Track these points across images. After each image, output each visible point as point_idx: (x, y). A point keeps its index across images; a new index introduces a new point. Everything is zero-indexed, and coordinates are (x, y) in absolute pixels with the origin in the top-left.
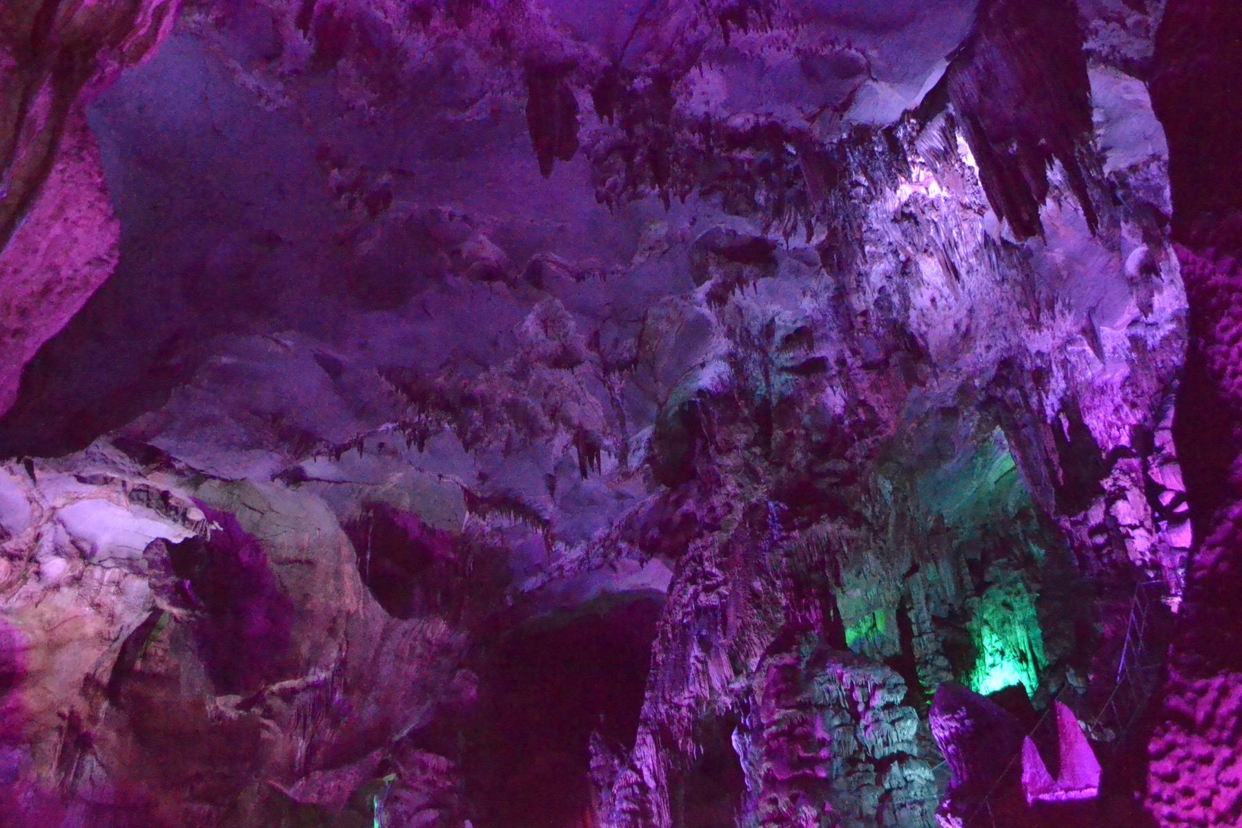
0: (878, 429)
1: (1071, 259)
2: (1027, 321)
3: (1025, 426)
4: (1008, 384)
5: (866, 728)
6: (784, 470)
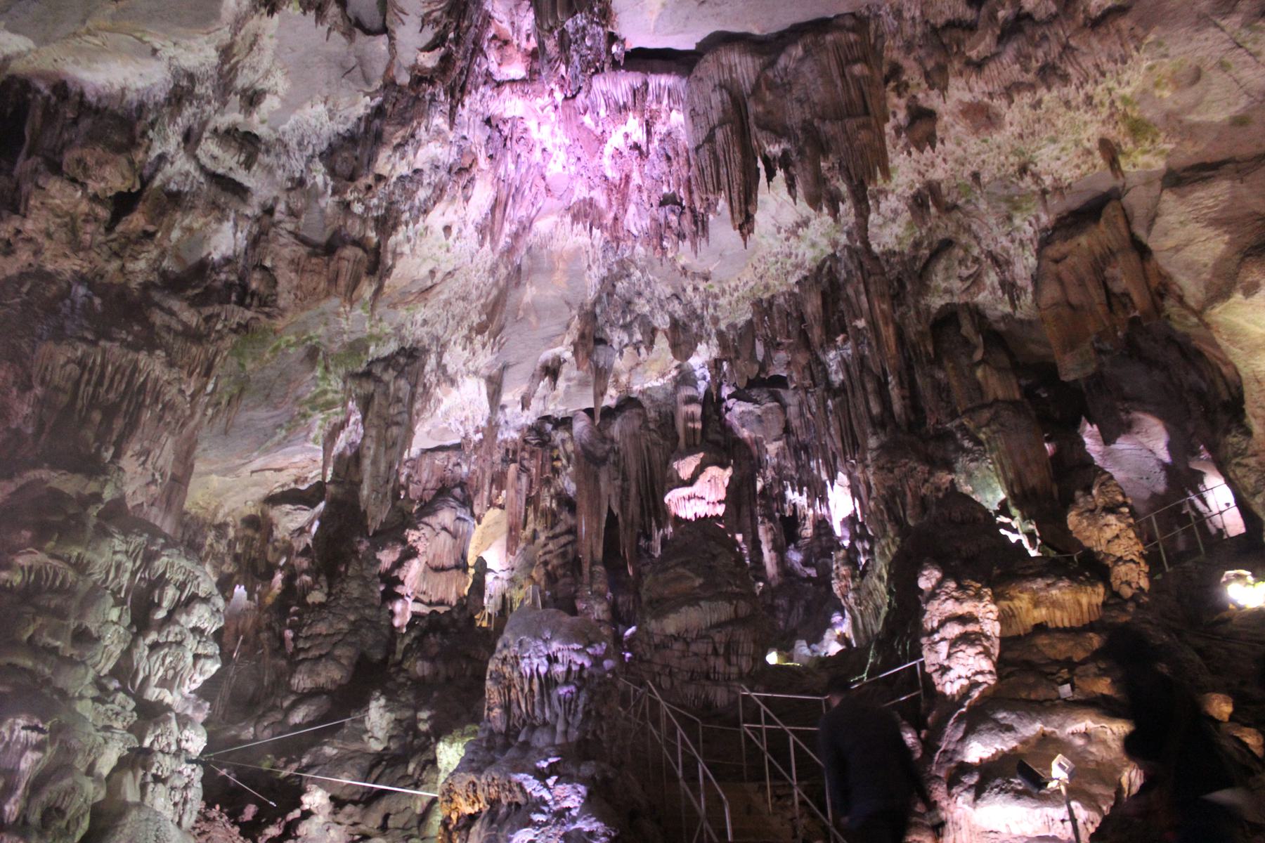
0: (267, 309)
1: (534, 308)
2: (471, 329)
3: (397, 424)
4: (400, 374)
5: (154, 647)
6: (115, 265)
